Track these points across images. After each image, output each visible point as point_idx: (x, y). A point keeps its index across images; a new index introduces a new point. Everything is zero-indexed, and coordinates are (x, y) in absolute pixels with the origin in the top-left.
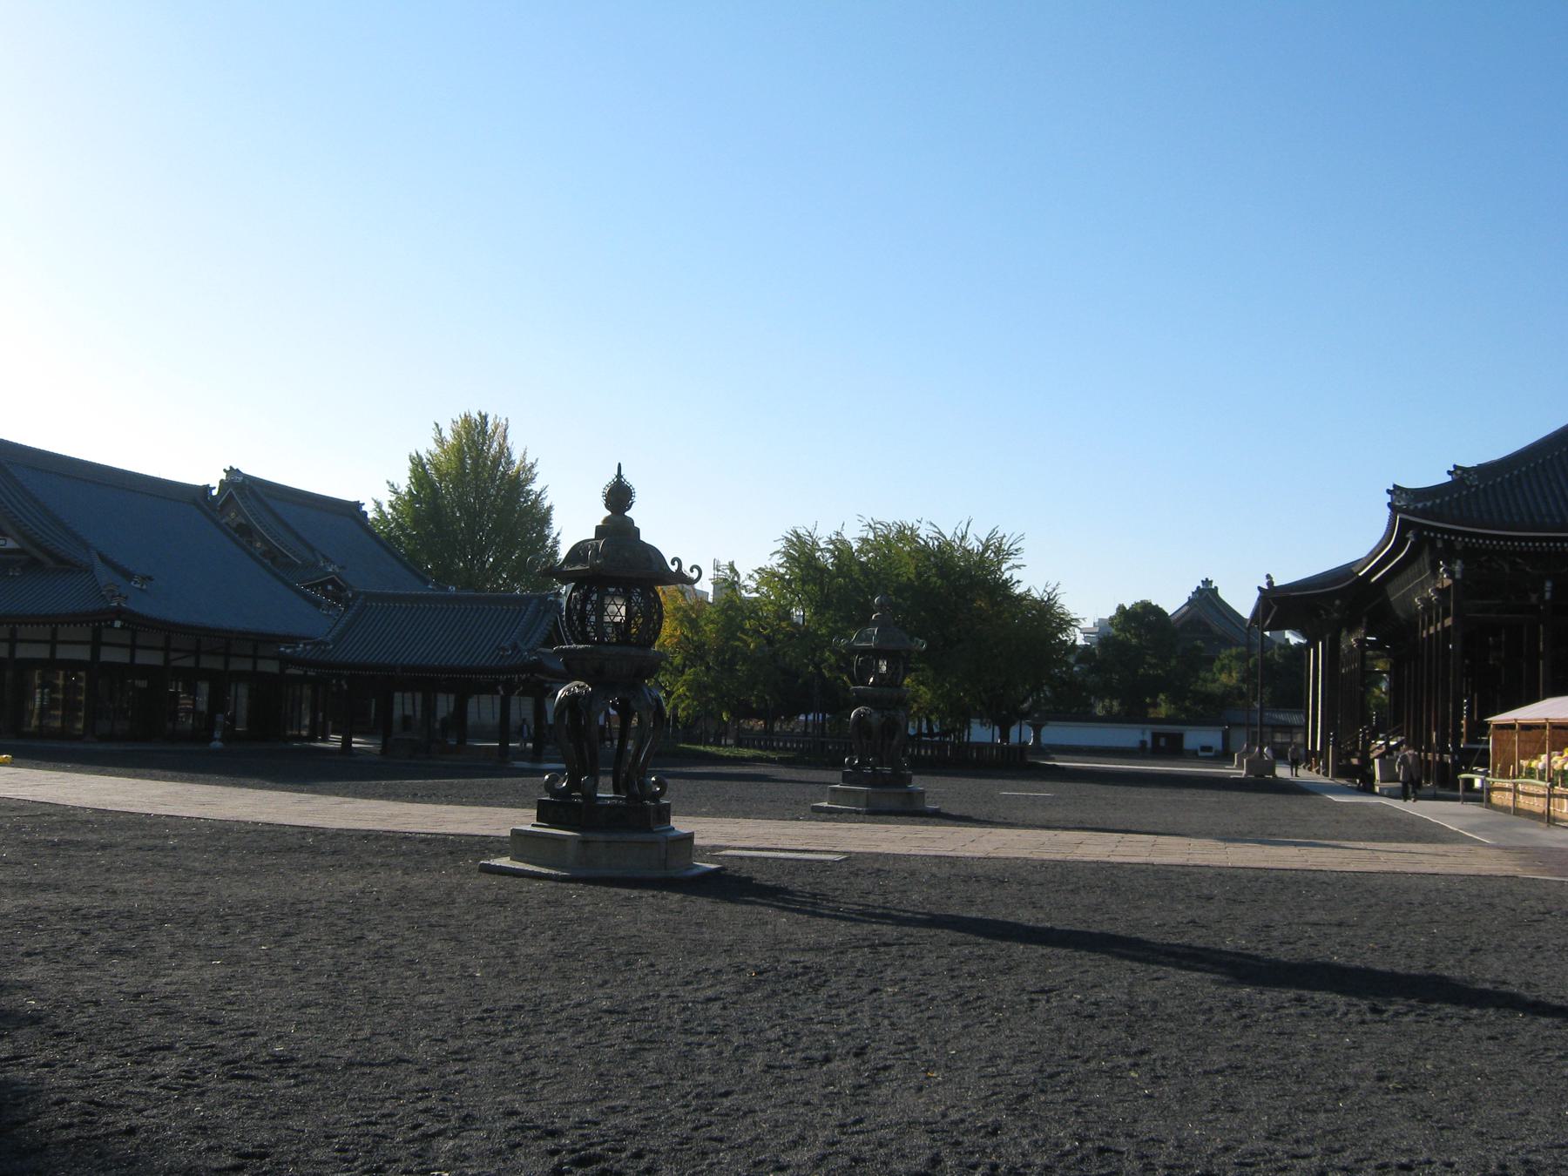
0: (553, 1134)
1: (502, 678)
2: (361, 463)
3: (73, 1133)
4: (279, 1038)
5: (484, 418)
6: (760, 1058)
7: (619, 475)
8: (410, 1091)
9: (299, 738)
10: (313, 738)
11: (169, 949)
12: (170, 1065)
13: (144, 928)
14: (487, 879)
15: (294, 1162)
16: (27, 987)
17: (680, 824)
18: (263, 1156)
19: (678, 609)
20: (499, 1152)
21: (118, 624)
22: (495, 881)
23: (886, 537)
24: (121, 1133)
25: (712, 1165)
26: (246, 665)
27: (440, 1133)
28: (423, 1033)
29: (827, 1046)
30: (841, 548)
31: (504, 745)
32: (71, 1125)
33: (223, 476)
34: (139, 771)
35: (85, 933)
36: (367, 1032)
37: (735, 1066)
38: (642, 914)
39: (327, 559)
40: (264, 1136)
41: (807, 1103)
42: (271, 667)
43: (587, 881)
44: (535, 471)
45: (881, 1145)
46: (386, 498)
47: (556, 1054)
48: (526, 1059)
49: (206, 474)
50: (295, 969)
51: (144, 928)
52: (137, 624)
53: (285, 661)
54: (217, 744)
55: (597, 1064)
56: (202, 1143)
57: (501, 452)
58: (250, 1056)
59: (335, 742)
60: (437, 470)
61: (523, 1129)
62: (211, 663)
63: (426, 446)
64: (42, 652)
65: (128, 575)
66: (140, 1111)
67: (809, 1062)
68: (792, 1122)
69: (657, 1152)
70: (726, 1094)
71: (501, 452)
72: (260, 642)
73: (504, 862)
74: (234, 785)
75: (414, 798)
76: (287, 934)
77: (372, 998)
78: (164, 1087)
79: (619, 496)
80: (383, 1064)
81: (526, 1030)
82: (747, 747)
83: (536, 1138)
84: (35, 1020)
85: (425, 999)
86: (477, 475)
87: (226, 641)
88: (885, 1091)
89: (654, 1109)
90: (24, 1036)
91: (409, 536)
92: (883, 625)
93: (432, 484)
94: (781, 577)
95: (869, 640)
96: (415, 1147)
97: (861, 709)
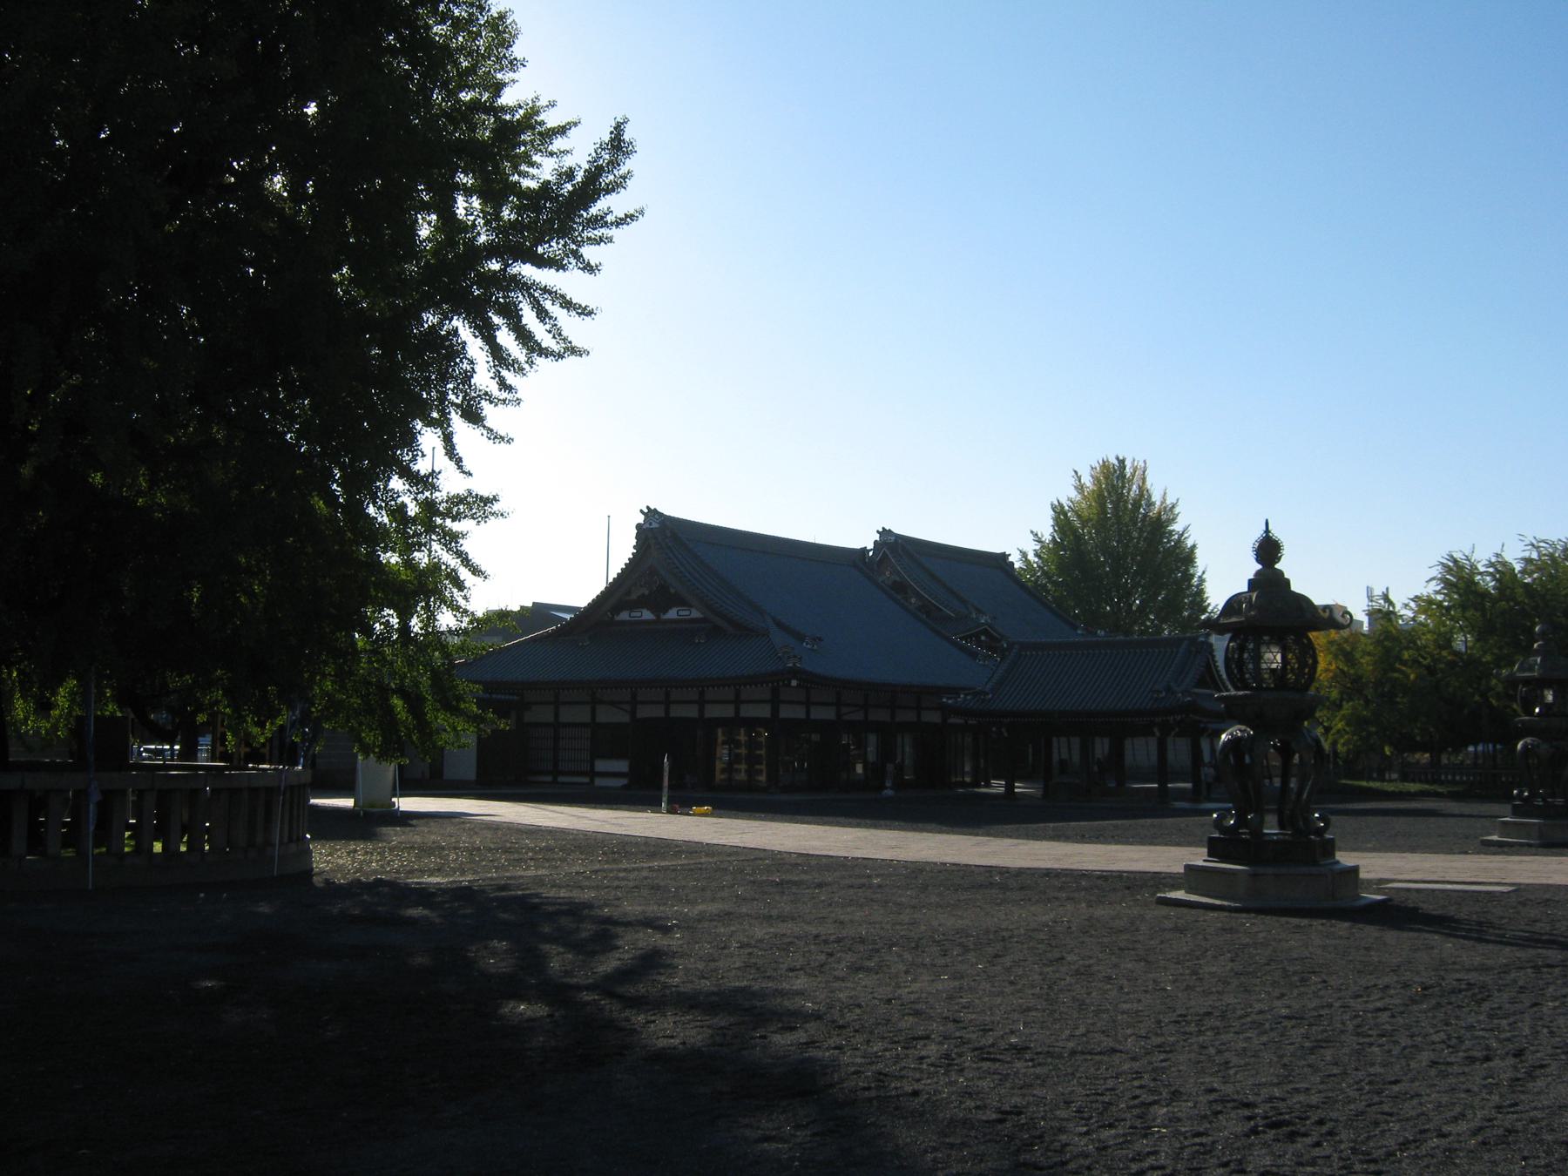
0: (1247, 1105)
1: (1159, 720)
2: (1004, 515)
3: (873, 1093)
4: (1012, 1032)
5: (1122, 462)
6: (1425, 1056)
7: (1267, 531)
8: (1125, 1072)
9: (963, 784)
10: (979, 786)
11: (902, 967)
12: (932, 1050)
13: (877, 951)
14: (1164, 910)
15: (1043, 1118)
16: (800, 993)
17: (1345, 859)
18: (1020, 1113)
20: (1205, 1117)
21: (794, 683)
22: (1173, 912)
23: (1551, 556)
24: (906, 1094)
25: (1383, 1132)
26: (910, 716)
27: (1155, 1103)
28: (1129, 1031)
29: (1488, 1048)
30: (1502, 571)
31: (1163, 784)
32: (869, 1089)
33: (877, 537)
35: (831, 955)
36: (1082, 1030)
37: (1403, 1062)
38: (1315, 939)
39: (979, 611)
40: (1016, 1100)
41: (1468, 1091)
42: (933, 717)
43: (1260, 911)
44: (1176, 511)
45: (1532, 1121)
46: (1031, 547)
47: (1244, 1049)
48: (1219, 1052)
49: (864, 539)
50: (1012, 983)
51: (877, 951)
52: (810, 681)
55: (1281, 1057)
56: (970, 1103)
57: (1141, 495)
58: (993, 1045)
59: (998, 786)
60: (1079, 517)
61: (1223, 1101)
62: (881, 715)
63: (1067, 494)
64: (727, 711)
65: (800, 637)
66: (918, 1081)
67: (1471, 1060)
68: (1454, 1104)
69: (1336, 1121)
70: (1396, 1082)
71: (1141, 495)
73: (1179, 895)
74: (914, 830)
75: (1082, 838)
76: (996, 956)
77: (1082, 1006)
78: (932, 1065)
79: (1268, 550)
80: (1100, 1053)
81: (1217, 1031)
82: (1413, 781)
83: (1234, 1108)
84: (817, 1016)
85: (1125, 1006)
88: (1540, 1083)
89: (1332, 1090)
90: (812, 1027)
91: (1055, 583)
93: (1074, 531)
94: (1439, 604)
95: (1531, 669)
96: (1136, 1112)
97: (1528, 740)
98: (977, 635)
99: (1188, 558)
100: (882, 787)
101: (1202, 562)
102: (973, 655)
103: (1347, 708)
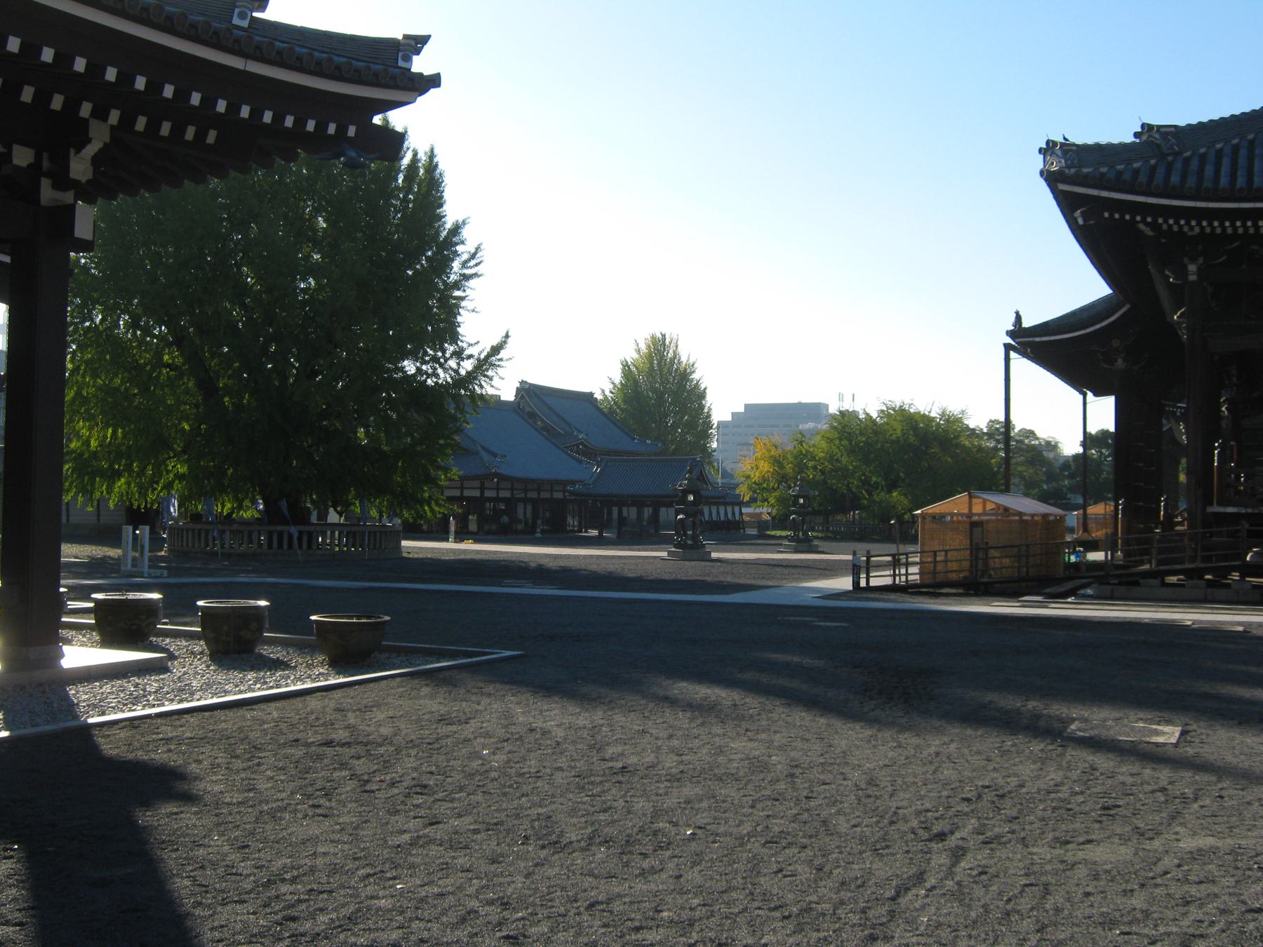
5: (664, 336)
9: (573, 531)
42: (558, 495)
46: (608, 387)
52: (502, 478)
53: (571, 493)
57: (675, 357)
59: (594, 533)
63: (631, 355)
65: (495, 455)
71: (675, 357)
72: (553, 484)
86: (661, 370)
87: (539, 485)
91: (621, 410)
98: (577, 445)
99: (702, 395)
100: (534, 532)
102: (580, 462)
103: (777, 494)
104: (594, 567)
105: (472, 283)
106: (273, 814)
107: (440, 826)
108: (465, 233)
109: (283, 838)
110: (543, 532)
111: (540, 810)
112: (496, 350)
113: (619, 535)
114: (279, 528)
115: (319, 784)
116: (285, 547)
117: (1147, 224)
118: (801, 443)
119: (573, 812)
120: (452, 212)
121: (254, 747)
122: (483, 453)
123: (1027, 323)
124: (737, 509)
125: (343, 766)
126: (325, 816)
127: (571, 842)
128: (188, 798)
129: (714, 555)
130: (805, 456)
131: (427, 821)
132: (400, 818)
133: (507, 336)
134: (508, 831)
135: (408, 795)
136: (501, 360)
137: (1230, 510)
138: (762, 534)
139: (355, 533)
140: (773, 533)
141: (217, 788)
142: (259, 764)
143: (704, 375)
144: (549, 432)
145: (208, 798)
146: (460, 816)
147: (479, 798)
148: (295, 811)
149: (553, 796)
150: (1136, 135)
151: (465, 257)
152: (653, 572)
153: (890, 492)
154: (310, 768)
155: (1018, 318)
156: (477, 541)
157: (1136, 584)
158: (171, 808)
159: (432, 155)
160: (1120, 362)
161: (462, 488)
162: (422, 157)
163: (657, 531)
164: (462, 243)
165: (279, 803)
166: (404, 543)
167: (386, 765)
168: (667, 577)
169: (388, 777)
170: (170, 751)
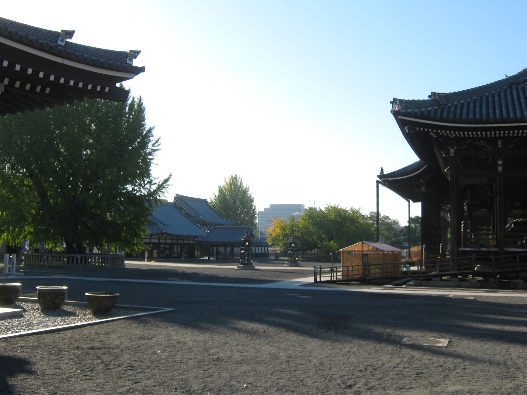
5: (236, 176)
9: (198, 257)
19: (281, 226)
34: (150, 268)
42: (191, 242)
46: (213, 197)
52: (168, 234)
53: (197, 241)
54: (183, 259)
57: (241, 185)
59: (206, 258)
63: (223, 184)
65: (165, 225)
71: (241, 185)
72: (189, 237)
87: (183, 237)
91: (218, 206)
92: (293, 239)
98: (200, 221)
99: (252, 201)
100: (181, 257)
101: (255, 203)
102: (201, 228)
104: (206, 273)
105: (156, 153)
106: (68, 379)
107: (140, 384)
108: (154, 132)
109: (72, 390)
110: (185, 257)
111: (182, 377)
112: (166, 181)
113: (216, 260)
114: (72, 255)
115: (88, 366)
116: (75, 263)
117: (434, 133)
118: (293, 221)
119: (196, 377)
120: (148, 124)
121: (60, 350)
122: (160, 224)
123: (386, 172)
124: (266, 248)
125: (98, 358)
126: (90, 380)
127: (195, 391)
128: (31, 372)
129: (257, 268)
130: (295, 226)
131: (133, 382)
132: (122, 380)
133: (171, 175)
134: (168, 386)
135: (126, 371)
136: (168, 185)
137: (468, 249)
138: (277, 259)
139: (105, 257)
140: (281, 258)
141: (43, 368)
142: (61, 357)
143: (252, 193)
144: (188, 215)
145: (39, 372)
146: (148, 379)
147: (156, 371)
148: (77, 378)
149: (188, 370)
150: (429, 97)
151: (154, 142)
152: (231, 275)
153: (330, 241)
154: (84, 359)
155: (382, 170)
156: (157, 261)
157: (431, 280)
158: (23, 376)
159: (140, 100)
160: (423, 189)
161: (151, 239)
162: (137, 100)
163: (233, 257)
164: (153, 136)
165: (70, 374)
166: (126, 262)
167: (117, 357)
168: (237, 277)
169: (117, 363)
170: (23, 351)
